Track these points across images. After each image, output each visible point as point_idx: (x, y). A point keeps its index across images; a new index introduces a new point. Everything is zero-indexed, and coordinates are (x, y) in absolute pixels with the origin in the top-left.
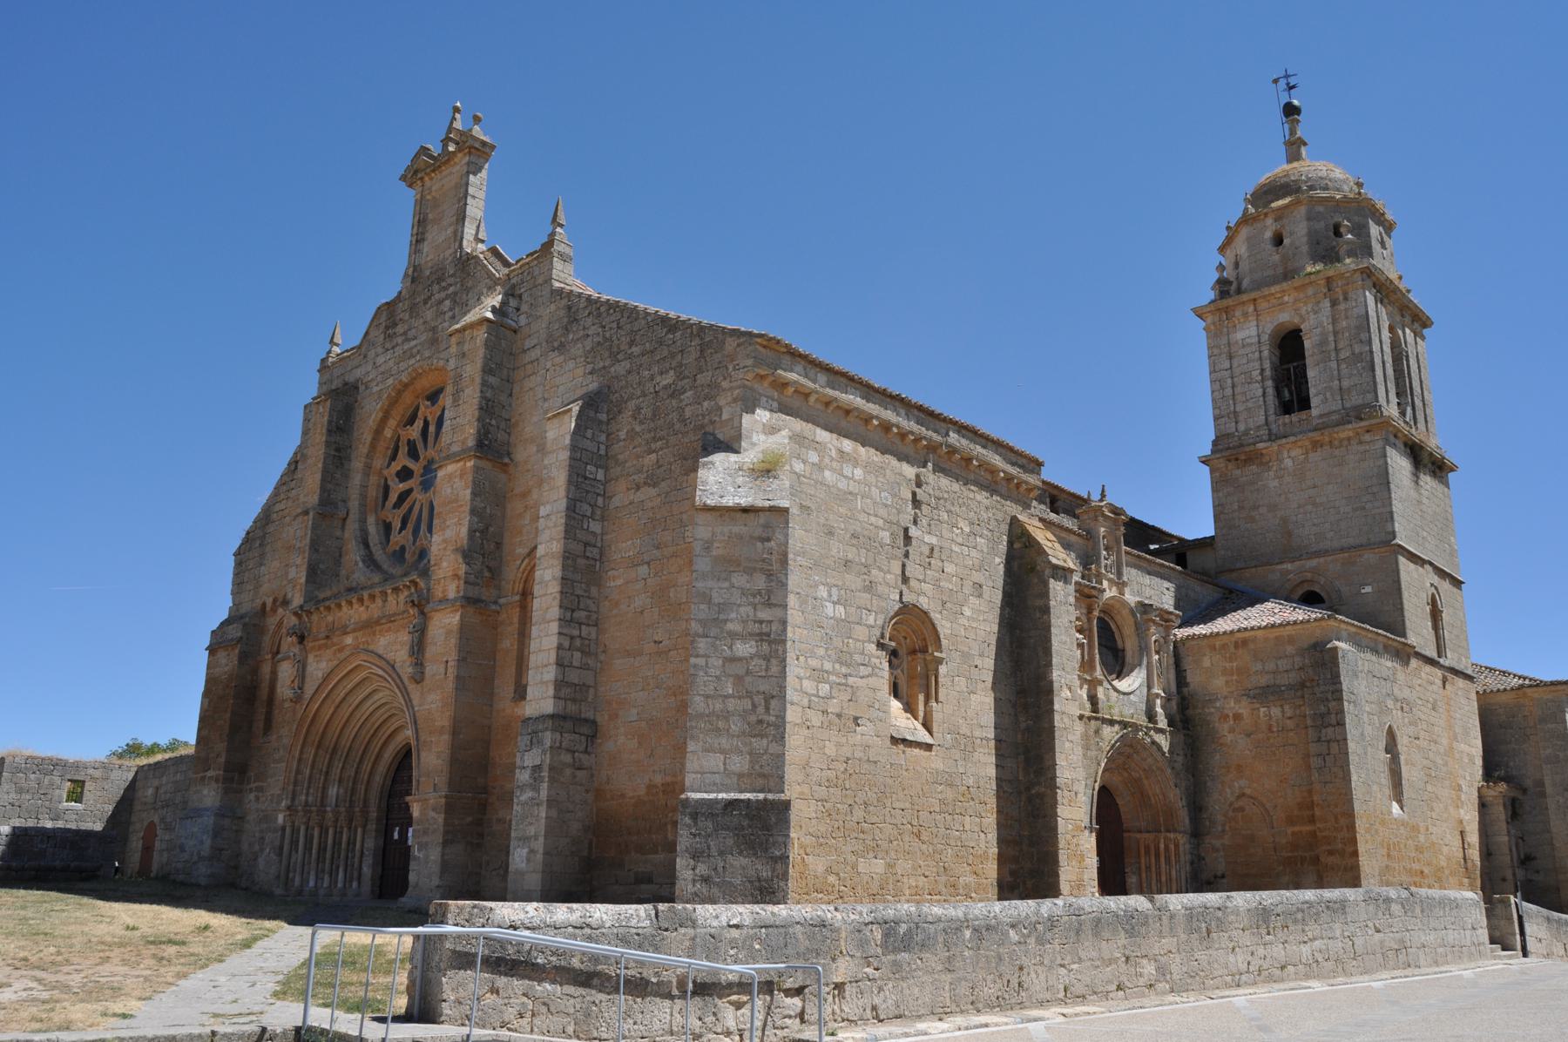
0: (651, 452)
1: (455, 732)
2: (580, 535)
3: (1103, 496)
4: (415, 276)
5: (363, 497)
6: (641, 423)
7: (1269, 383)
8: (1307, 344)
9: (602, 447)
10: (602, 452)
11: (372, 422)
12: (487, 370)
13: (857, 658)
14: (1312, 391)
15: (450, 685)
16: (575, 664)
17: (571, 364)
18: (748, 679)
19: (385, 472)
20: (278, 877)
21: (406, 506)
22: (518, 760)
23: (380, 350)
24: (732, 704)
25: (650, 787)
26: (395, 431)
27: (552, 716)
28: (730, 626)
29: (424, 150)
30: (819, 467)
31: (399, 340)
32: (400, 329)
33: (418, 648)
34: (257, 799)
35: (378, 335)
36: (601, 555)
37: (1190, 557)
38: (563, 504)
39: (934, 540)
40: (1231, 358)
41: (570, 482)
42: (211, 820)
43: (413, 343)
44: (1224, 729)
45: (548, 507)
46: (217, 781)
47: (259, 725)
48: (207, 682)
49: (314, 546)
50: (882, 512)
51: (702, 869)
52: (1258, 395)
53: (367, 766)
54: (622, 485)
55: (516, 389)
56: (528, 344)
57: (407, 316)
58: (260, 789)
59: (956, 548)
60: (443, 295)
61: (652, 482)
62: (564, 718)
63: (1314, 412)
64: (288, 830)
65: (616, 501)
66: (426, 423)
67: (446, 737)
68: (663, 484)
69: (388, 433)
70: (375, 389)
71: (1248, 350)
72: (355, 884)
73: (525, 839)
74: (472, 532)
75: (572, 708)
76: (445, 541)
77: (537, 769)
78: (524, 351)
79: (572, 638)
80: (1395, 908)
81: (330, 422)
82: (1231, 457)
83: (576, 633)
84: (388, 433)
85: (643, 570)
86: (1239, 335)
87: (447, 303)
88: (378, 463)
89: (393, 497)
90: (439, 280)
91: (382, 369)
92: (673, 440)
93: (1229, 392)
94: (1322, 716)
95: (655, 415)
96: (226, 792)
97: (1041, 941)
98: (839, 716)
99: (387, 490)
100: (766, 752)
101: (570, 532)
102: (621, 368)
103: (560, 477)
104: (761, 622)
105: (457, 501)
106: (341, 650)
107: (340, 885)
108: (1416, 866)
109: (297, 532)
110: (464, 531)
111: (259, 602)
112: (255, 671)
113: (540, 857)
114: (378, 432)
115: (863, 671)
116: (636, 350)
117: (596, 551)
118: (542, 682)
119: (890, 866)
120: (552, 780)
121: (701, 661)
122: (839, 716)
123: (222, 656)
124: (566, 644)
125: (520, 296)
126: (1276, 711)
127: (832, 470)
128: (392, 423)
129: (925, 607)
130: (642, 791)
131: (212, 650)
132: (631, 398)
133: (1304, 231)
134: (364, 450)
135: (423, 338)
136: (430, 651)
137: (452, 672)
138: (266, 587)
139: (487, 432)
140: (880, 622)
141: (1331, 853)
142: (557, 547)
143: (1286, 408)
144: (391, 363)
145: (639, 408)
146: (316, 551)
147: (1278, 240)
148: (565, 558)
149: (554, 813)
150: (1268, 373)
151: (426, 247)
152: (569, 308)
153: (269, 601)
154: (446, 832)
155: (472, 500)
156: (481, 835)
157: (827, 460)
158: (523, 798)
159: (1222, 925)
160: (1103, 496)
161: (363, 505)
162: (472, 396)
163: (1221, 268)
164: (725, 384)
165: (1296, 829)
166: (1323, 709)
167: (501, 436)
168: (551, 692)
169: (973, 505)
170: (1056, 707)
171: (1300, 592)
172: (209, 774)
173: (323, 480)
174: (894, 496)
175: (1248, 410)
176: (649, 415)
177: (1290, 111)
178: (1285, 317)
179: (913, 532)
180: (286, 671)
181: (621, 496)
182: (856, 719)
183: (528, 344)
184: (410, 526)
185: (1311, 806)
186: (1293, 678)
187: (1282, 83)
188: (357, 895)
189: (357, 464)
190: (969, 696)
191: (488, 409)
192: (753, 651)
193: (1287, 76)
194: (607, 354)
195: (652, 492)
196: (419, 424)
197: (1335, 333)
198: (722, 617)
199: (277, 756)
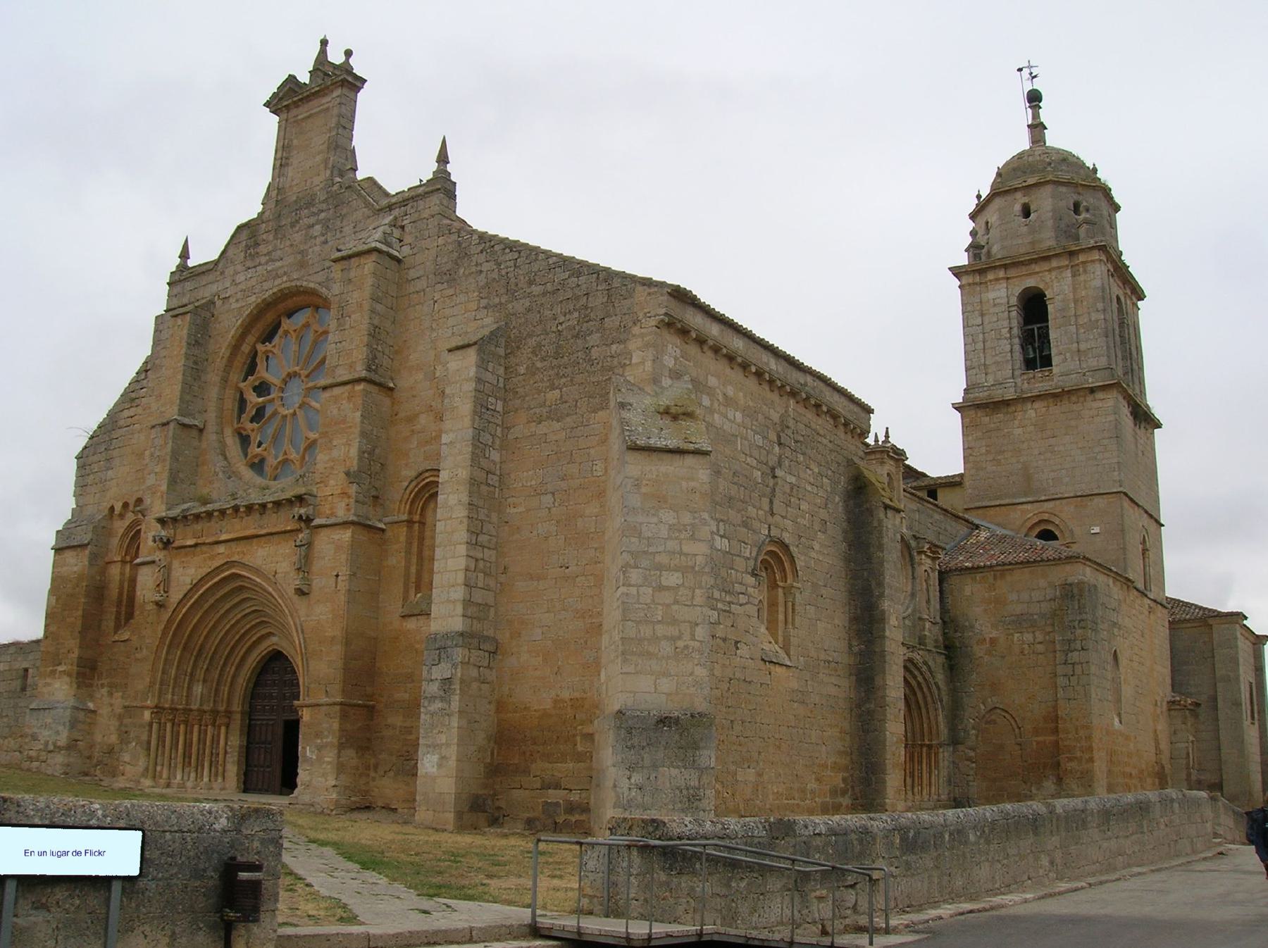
0: (553, 388)
1: (347, 643)
2: (484, 463)
3: (887, 436)
4: (276, 196)
6: (543, 360)
7: (1017, 341)
8: (1050, 308)
9: (501, 380)
10: (501, 385)
13: (738, 588)
14: (1054, 352)
15: (342, 598)
16: (480, 585)
18: (675, 607)
19: (242, 385)
20: (147, 769)
22: (425, 673)
23: (239, 268)
24: (661, 630)
25: (557, 701)
27: (462, 634)
28: (658, 558)
29: (292, 78)
30: (710, 410)
31: (263, 260)
32: (263, 249)
33: (304, 566)
35: (238, 254)
37: (940, 494)
38: (470, 433)
39: (793, 480)
40: (982, 315)
41: (475, 412)
42: (68, 712)
43: (279, 264)
44: (979, 651)
46: (69, 675)
47: (109, 623)
48: (53, 580)
49: (175, 455)
50: (756, 453)
51: (637, 778)
52: (1007, 347)
59: (809, 488)
60: (312, 220)
61: (555, 415)
62: (472, 635)
63: (1055, 370)
67: (338, 649)
68: (568, 419)
70: (234, 306)
71: (996, 310)
72: (220, 779)
73: (435, 746)
74: (361, 452)
75: (477, 626)
77: (447, 681)
80: (1176, 805)
81: (189, 335)
82: (977, 408)
83: (480, 555)
84: (246, 348)
85: (548, 499)
86: (991, 295)
87: (318, 227)
88: (235, 377)
90: (310, 204)
92: (578, 378)
93: (980, 346)
94: (1069, 641)
95: (557, 355)
97: (988, 842)
98: (724, 640)
99: (242, 402)
100: (691, 674)
101: (475, 459)
102: (520, 306)
103: (464, 406)
104: (686, 555)
105: (344, 421)
106: (212, 558)
108: (1128, 770)
110: (354, 452)
111: (106, 506)
112: (103, 572)
113: (452, 763)
114: (236, 348)
115: (743, 599)
116: (536, 289)
117: (496, 478)
118: (448, 601)
119: (760, 775)
121: (633, 590)
122: (724, 640)
123: (69, 556)
124: (472, 566)
125: (403, 227)
126: (1028, 637)
127: (722, 414)
128: (251, 339)
129: (787, 541)
130: (548, 705)
131: (58, 550)
132: (530, 336)
133: (1049, 208)
134: (220, 363)
135: (290, 260)
136: (317, 566)
137: (343, 585)
140: (754, 554)
141: (1070, 759)
142: (464, 474)
143: (1030, 364)
144: (253, 282)
145: (540, 346)
147: (1026, 212)
148: (472, 485)
150: (1016, 331)
151: (290, 172)
152: (460, 244)
153: (118, 507)
155: (362, 422)
157: (716, 405)
159: (1084, 824)
160: (887, 436)
162: (360, 322)
163: (973, 234)
164: (636, 330)
165: (1040, 739)
166: (1069, 636)
167: (386, 362)
169: (821, 448)
170: (887, 633)
171: (1037, 530)
172: (60, 668)
173: (183, 391)
174: (764, 438)
175: (997, 363)
177: (1034, 98)
178: (1031, 282)
179: (779, 472)
182: (737, 642)
183: (412, 274)
185: (1056, 719)
186: (1046, 607)
187: (1026, 71)
190: (822, 625)
191: (375, 333)
192: (680, 582)
193: (1030, 67)
194: (503, 291)
195: (557, 425)
197: (1076, 301)
198: (651, 549)
199: (138, 656)
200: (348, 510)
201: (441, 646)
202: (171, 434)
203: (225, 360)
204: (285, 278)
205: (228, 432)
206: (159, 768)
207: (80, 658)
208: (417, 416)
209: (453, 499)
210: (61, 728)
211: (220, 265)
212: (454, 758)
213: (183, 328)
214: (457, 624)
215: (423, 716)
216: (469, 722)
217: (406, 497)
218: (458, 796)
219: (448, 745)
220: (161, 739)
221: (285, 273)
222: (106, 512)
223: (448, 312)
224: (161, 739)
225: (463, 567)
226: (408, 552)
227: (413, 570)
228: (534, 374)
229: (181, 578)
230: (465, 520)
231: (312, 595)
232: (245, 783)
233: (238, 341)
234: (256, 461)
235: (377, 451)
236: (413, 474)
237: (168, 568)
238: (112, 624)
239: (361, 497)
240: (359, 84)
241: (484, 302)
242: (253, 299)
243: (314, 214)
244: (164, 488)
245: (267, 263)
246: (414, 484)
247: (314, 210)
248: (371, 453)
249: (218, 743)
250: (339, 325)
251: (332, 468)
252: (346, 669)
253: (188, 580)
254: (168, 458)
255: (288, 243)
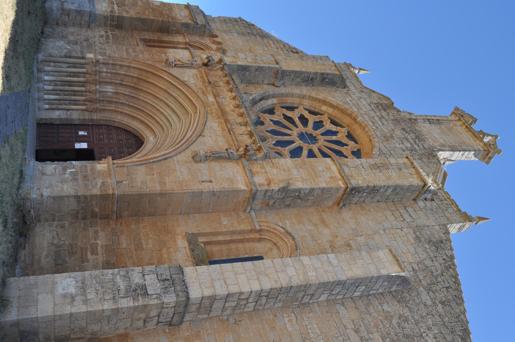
5: (287, 95)
6: (399, 324)
9: (374, 292)
11: (330, 99)
12: (396, 188)
15: (196, 187)
16: (227, 304)
17: (412, 250)
19: (301, 108)
20: (51, 56)
21: (287, 123)
23: (368, 101)
26: (326, 112)
27: (188, 298)
29: (475, 120)
31: (378, 114)
32: (384, 113)
33: (215, 157)
34: (101, 36)
36: (305, 304)
43: (379, 122)
45: (335, 262)
46: (111, 12)
47: (147, 36)
48: (169, 4)
49: (259, 69)
53: (127, 110)
54: (355, 315)
55: (383, 205)
56: (410, 210)
57: (392, 117)
58: (108, 37)
60: (412, 141)
62: (186, 306)
64: (82, 61)
65: (342, 310)
66: (335, 133)
69: (324, 108)
70: (348, 99)
72: (47, 106)
73: (83, 288)
74: (299, 191)
75: (193, 308)
76: (289, 170)
78: (405, 208)
79: (247, 299)
81: (328, 74)
83: (250, 300)
84: (324, 108)
87: (409, 145)
88: (307, 103)
89: (289, 114)
91: (360, 103)
96: (106, 17)
99: (291, 109)
106: (204, 93)
107: (46, 97)
109: (260, 57)
111: (217, 33)
112: (178, 32)
113: (68, 310)
114: (324, 102)
118: (213, 281)
120: (135, 308)
123: (185, 13)
125: (432, 200)
128: (330, 110)
131: (188, 7)
134: (314, 94)
136: (215, 165)
137: (206, 187)
138: (225, 35)
139: (359, 192)
144: (364, 109)
145: (406, 320)
146: (257, 70)
148: (305, 286)
149: (106, 314)
151: (427, 125)
152: (442, 242)
153: (219, 39)
154: (85, 197)
155: (319, 189)
156: (84, 218)
158: (119, 280)
161: (282, 95)
167: (356, 199)
168: (207, 293)
172: (116, 7)
173: (296, 72)
176: (407, 331)
180: (183, 55)
181: (347, 314)
184: (276, 128)
188: (39, 109)
189: (305, 90)
191: (373, 190)
196: (334, 128)
199: (130, 50)
200: (260, 185)
201: (176, 281)
202: (272, 66)
203: (316, 96)
204: (374, 127)
205: (275, 101)
206: (52, 64)
207: (123, 18)
208: (327, 226)
209: (291, 271)
210: (76, 5)
211: (365, 90)
212: (74, 310)
213: (331, 70)
214: (195, 293)
215: (110, 271)
216: (109, 317)
217: (272, 226)
218: (32, 320)
219: (86, 302)
220: (74, 65)
221: (377, 127)
222: (214, 33)
223: (399, 239)
224: (74, 65)
225: (243, 290)
226: (233, 233)
227: (221, 238)
228: (386, 318)
229: (186, 75)
230: (278, 286)
231: (194, 163)
232: (45, 124)
233: (328, 103)
234: (262, 119)
235: (299, 201)
236: (289, 230)
237: (190, 66)
238: (147, 37)
239: (269, 193)
240: (486, 160)
241: (416, 267)
242: (356, 110)
243: (415, 142)
244: (239, 63)
245: (377, 116)
246: (282, 230)
247: (417, 142)
248: (299, 197)
249: (75, 105)
250: (373, 165)
251: (284, 170)
252: (141, 196)
253: (186, 79)
254: (258, 65)
255: (393, 128)
